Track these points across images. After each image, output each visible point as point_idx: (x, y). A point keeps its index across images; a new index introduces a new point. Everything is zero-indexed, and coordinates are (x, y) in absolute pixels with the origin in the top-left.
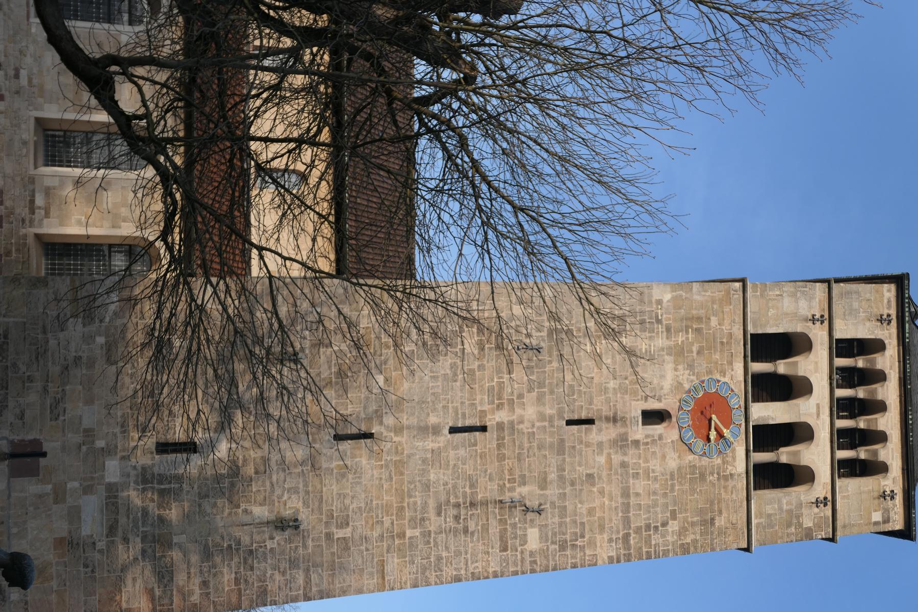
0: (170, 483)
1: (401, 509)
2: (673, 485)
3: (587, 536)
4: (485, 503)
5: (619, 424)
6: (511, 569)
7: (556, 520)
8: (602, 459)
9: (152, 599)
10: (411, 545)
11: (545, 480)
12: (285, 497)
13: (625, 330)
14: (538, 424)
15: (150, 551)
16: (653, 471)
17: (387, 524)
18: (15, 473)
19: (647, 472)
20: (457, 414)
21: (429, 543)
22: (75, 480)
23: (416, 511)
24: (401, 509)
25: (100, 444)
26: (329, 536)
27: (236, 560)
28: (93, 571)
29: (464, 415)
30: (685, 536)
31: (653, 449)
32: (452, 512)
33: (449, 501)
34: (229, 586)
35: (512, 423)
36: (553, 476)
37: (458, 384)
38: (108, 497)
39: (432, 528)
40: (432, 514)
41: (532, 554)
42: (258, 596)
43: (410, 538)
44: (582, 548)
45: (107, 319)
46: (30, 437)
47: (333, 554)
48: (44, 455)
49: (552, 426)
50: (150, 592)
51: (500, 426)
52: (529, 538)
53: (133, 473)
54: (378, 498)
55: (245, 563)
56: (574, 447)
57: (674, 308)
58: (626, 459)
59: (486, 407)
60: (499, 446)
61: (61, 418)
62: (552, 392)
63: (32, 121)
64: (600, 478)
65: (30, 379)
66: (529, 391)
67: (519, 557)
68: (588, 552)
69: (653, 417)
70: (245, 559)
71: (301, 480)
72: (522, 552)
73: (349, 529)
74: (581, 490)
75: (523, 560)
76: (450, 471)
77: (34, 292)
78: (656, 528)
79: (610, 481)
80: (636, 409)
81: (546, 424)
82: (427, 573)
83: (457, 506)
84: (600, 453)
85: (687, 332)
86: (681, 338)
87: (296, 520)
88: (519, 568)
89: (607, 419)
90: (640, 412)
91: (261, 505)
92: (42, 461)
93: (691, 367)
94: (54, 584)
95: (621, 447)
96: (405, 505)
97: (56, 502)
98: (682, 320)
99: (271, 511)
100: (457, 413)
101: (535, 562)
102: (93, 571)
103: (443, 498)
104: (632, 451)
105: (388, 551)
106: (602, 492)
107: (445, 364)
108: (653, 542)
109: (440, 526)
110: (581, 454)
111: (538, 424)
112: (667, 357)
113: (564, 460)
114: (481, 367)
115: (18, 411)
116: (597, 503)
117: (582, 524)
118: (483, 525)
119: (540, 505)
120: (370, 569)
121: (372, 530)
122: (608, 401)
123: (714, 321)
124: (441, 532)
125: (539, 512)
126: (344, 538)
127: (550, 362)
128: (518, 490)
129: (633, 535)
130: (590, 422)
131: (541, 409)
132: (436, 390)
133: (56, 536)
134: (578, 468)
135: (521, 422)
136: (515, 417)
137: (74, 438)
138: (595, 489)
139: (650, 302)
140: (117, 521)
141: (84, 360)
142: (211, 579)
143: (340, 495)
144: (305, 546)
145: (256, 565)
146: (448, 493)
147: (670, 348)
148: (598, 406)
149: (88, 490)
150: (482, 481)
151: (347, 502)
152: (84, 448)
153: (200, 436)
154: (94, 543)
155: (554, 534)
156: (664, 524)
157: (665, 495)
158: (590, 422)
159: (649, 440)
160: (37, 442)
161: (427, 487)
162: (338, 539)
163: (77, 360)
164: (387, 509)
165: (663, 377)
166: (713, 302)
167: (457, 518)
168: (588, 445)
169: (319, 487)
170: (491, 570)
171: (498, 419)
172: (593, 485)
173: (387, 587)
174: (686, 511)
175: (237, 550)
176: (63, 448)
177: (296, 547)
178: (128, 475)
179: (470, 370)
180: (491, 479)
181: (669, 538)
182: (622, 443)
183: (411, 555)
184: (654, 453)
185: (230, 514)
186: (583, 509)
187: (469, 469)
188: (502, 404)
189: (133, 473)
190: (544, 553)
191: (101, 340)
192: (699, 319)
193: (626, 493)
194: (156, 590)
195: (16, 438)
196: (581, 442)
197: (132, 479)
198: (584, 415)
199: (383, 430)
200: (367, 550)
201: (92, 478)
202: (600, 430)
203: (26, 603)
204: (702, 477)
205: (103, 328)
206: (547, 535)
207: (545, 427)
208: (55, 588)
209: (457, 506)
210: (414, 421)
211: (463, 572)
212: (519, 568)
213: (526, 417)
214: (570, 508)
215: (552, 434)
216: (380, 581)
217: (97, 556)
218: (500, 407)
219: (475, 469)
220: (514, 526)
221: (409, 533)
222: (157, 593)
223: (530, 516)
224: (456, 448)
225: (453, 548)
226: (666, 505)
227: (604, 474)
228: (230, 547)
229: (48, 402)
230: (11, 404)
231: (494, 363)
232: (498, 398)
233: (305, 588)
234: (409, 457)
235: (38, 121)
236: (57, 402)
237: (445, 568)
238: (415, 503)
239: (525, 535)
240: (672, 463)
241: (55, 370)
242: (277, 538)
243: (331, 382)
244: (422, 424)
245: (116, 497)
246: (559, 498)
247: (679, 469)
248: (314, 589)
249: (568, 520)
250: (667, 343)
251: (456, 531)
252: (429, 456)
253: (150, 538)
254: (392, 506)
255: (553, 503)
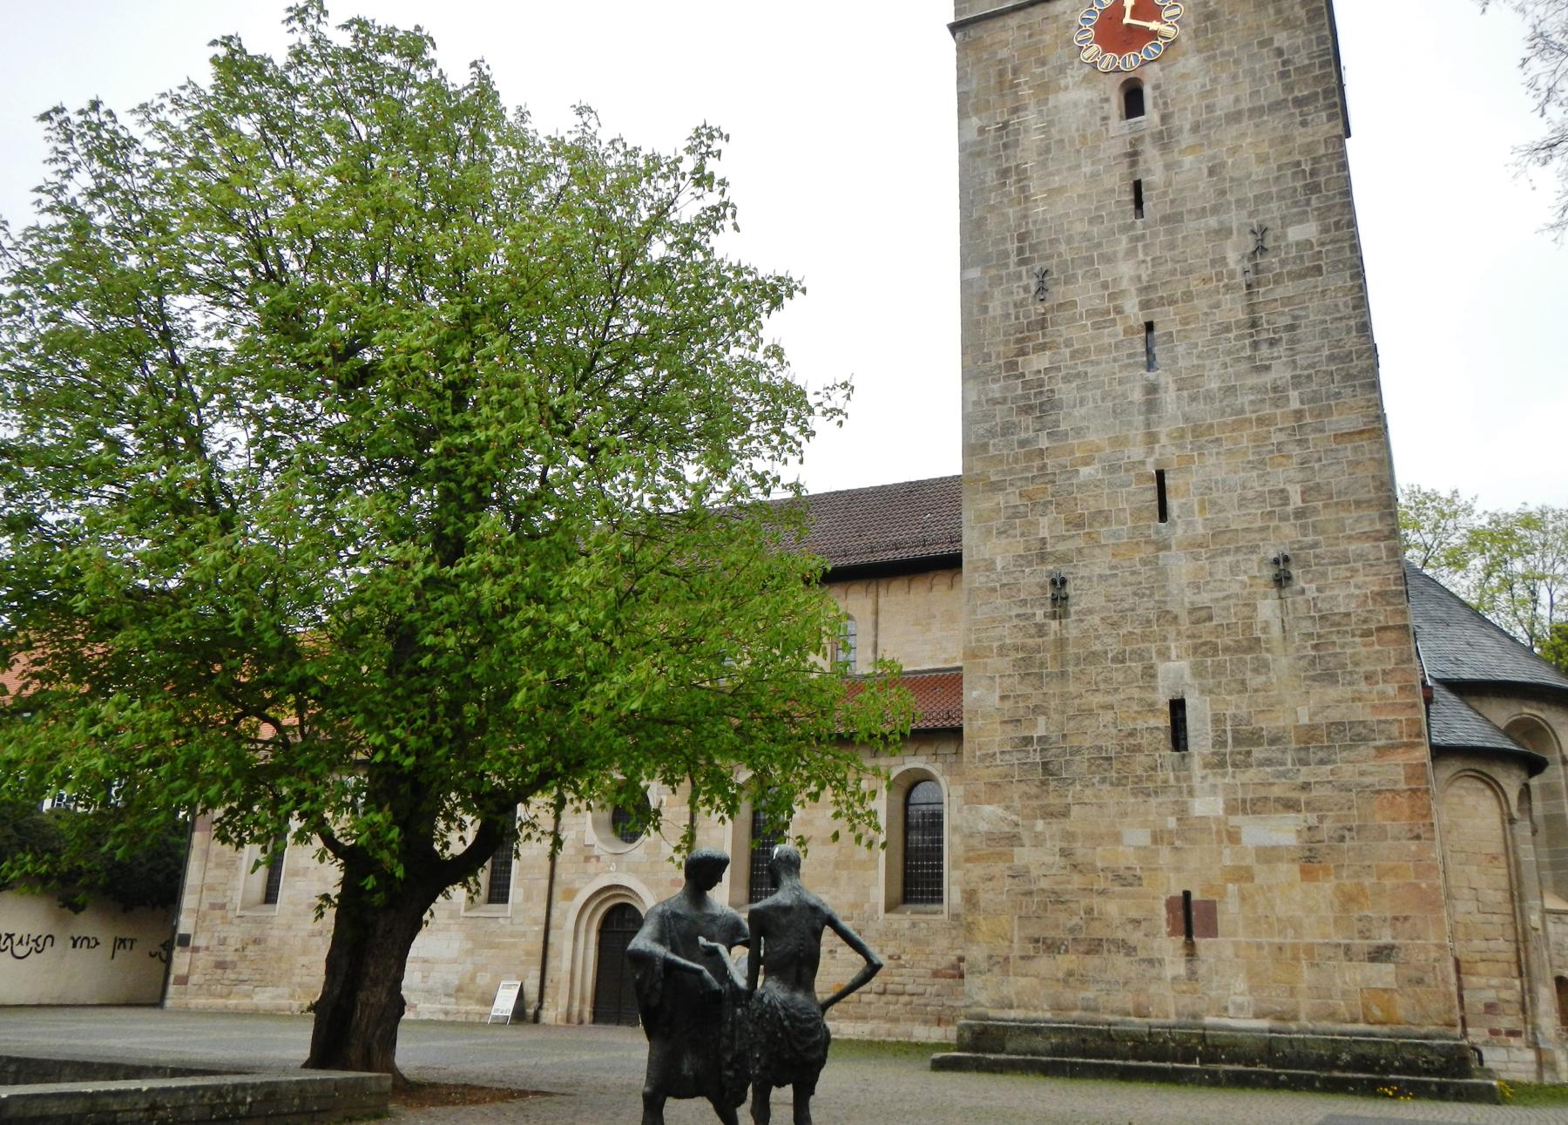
0: (1225, 731)
1: (1261, 421)
2: (1223, 54)
3: (1297, 158)
4: (1252, 308)
5: (1139, 148)
6: (1348, 254)
7: (1274, 205)
8: (1188, 160)
9: (1393, 748)
10: (1312, 400)
11: (1217, 232)
12: (1245, 578)
13: (1017, 166)
14: (1141, 256)
15: (1321, 754)
16: (1204, 86)
17: (1282, 437)
18: (1211, 930)
19: (1206, 94)
20: (1129, 365)
21: (1309, 377)
22: (1221, 853)
23: (1263, 401)
24: (1261, 421)
25: (1172, 823)
26: (1300, 514)
27: (1334, 638)
28: (1350, 830)
29: (1130, 356)
30: (1297, 19)
31: (1172, 93)
32: (1264, 350)
33: (1249, 358)
34: (1372, 644)
35: (1140, 291)
36: (1213, 222)
37: (1089, 370)
38: (1244, 811)
39: (1288, 375)
40: (1267, 379)
41: (1326, 230)
42: (1388, 604)
43: (1302, 402)
44: (1316, 160)
45: (1015, 818)
46: (1163, 912)
47: (1326, 506)
48: (1187, 894)
49: (1143, 236)
50: (1381, 752)
51: (1145, 305)
52: (1301, 237)
53: (1211, 780)
54: (1245, 454)
55: (1339, 624)
56: (1172, 202)
57: (987, 109)
58: (1187, 127)
59: (1120, 328)
60: (1172, 302)
61: (1138, 872)
62: (1099, 245)
63: (889, 916)
64: (1214, 157)
65: (1089, 911)
66: (1097, 275)
67: (1329, 247)
68: (1322, 151)
69: (1133, 100)
70: (1332, 625)
71: (1219, 559)
72: (1323, 244)
73: (1289, 488)
74: (1232, 180)
75: (1332, 241)
76: (1207, 362)
77: (982, 905)
78: (1284, 63)
79: (1220, 142)
80: (1119, 126)
81: (1140, 245)
82: (1354, 372)
83: (1255, 345)
84: (1179, 164)
85: (1018, 85)
86: (1025, 92)
87: (1276, 562)
88: (1346, 244)
89: (1133, 164)
90: (1124, 123)
91: (1255, 610)
92: (1196, 896)
93: (1061, 70)
94: (1368, 881)
95: (1170, 137)
96: (1254, 416)
97: (1251, 878)
98: (1002, 96)
99: (1265, 596)
100: (1129, 365)
101: (1337, 224)
102: (1350, 830)
103: (1244, 366)
104: (1176, 122)
105: (1322, 431)
106: (1234, 151)
107: (1065, 391)
108: (1306, 62)
109: (1285, 364)
110: (1182, 190)
111: (1141, 256)
112: (1050, 104)
113: (1190, 211)
114: (1068, 343)
115: (1129, 927)
116: (1249, 154)
117: (1280, 168)
118: (1283, 305)
119: (1253, 232)
120: (1349, 452)
121: (1289, 457)
122: (1108, 169)
123: (1003, 53)
124: (1294, 362)
125: (1264, 231)
126: (1303, 493)
127: (1060, 255)
128: (1232, 265)
129: (1297, 93)
130: (1137, 187)
131: (1121, 255)
132: (1098, 397)
133: (1298, 876)
134: (1200, 190)
135: (1139, 278)
136: (1133, 289)
137: (1165, 855)
138: (1230, 161)
139: (981, 142)
140: (1277, 800)
141: (1064, 845)
142: (1361, 670)
143: (1240, 506)
144: (1315, 545)
145: (1342, 610)
146: (1238, 360)
147: (1038, 103)
148: (1117, 180)
149: (1234, 837)
150: (1219, 317)
151: (1250, 494)
152: (1178, 843)
153: (1163, 699)
154: (1309, 829)
155: (1296, 204)
156: (1279, 52)
157: (1237, 62)
158: (1137, 187)
159: (1160, 102)
160: (1170, 904)
161: (1230, 390)
162: (1303, 501)
163: (1065, 853)
164: (1259, 441)
165: (1075, 105)
166: (979, 60)
167: (1273, 343)
168: (1169, 184)
169: (1229, 535)
170: (1349, 284)
171: (1137, 309)
172: (1223, 165)
173: (1376, 425)
174: (1259, 27)
175: (1319, 636)
176: (1178, 869)
177: (1316, 556)
178: (1215, 786)
179: (1072, 357)
180: (1217, 306)
181: (1299, 41)
182: (1164, 139)
183: (1328, 398)
184: (1178, 91)
185: (1268, 650)
186: (1258, 171)
187: (1202, 339)
188: (1115, 308)
189: (1211, 780)
190: (1322, 213)
191: (1040, 825)
192: (1001, 74)
193: (1234, 117)
194: (1378, 743)
195: (1165, 929)
196: (1165, 193)
197: (1219, 781)
198: (1129, 197)
199: (1151, 460)
200: (1320, 459)
201: (1218, 832)
202: (1148, 171)
203: (1396, 919)
204: (1210, 16)
205: (1026, 822)
206: (1299, 214)
207: (1145, 247)
208: (1374, 880)
209: (1255, 345)
210: (1139, 419)
211: (1352, 323)
212: (1346, 244)
213: (1132, 273)
214: (1257, 190)
215: (1155, 235)
216: (1366, 436)
217: (1327, 825)
218: (1119, 310)
219: (1204, 329)
220: (1283, 262)
221: (1295, 404)
222: (1381, 742)
223: (1269, 243)
224: (1175, 360)
225: (1317, 342)
226: (1252, 57)
227: (1208, 152)
228: (1315, 647)
229: (1118, 889)
230: (1120, 935)
231: (1062, 328)
232: (1102, 319)
233: (1377, 539)
234: (1187, 419)
235: (889, 908)
236: (1118, 877)
237: (1347, 348)
238: (1252, 402)
239: (1298, 244)
240: (1192, 62)
241: (1077, 880)
242: (1302, 584)
243: (1089, 534)
244: (1143, 409)
245: (1244, 801)
246: (1243, 207)
247: (1199, 51)
248: (1378, 526)
249: (1274, 189)
250: (1032, 107)
251: (1293, 341)
252: (1185, 393)
253: (1303, 754)
254: (1256, 434)
255: (1251, 215)
